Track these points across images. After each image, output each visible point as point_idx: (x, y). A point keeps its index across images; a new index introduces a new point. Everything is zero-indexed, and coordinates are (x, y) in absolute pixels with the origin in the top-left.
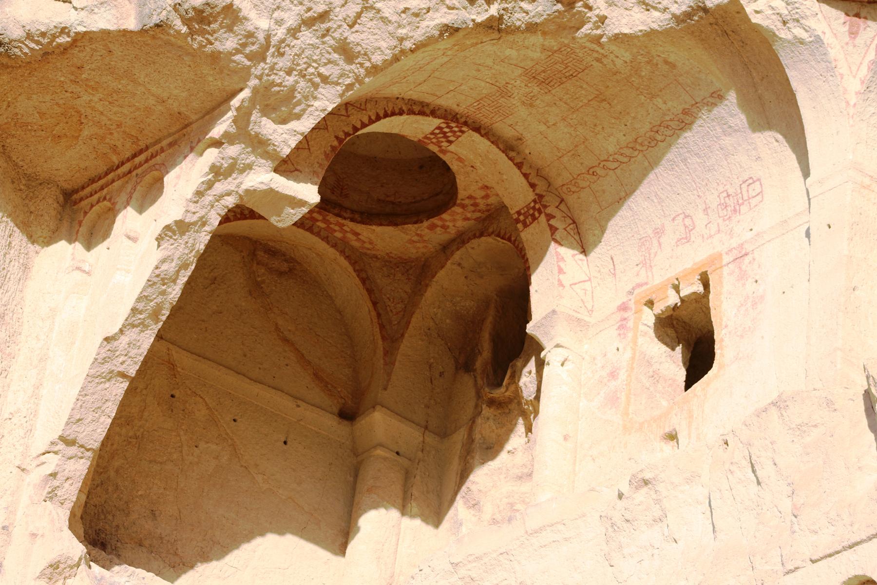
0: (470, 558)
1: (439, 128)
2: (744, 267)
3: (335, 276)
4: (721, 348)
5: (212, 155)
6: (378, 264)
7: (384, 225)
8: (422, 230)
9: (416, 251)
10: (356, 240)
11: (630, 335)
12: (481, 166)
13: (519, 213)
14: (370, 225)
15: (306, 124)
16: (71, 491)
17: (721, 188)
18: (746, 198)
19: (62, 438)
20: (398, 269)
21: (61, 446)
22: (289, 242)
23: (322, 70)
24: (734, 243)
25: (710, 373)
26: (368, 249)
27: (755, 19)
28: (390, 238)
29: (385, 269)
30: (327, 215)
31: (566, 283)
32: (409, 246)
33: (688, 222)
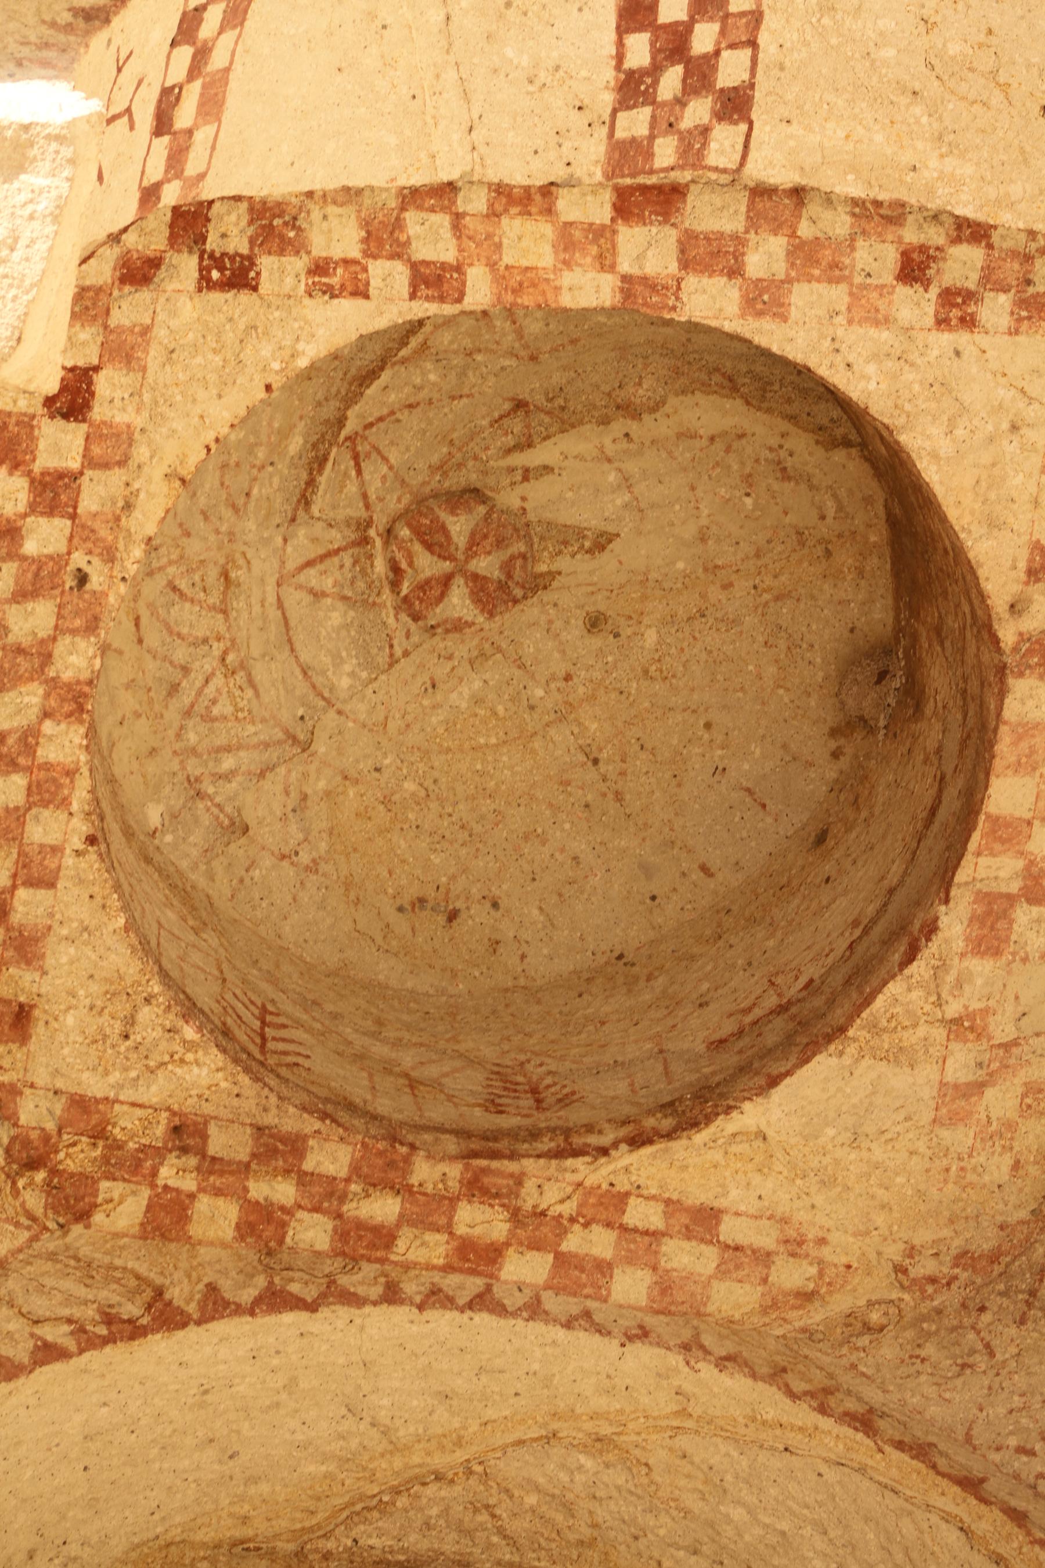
3: (738, 1514)
6: (888, 1350)
7: (788, 1073)
8: (959, 984)
9: (1008, 1160)
10: (722, 1272)
12: (950, 163)
14: (728, 1110)
20: (986, 1318)
22: (439, 1461)
26: (806, 1297)
28: (854, 1142)
29: (929, 1350)
30: (519, 1180)
32: (959, 1138)
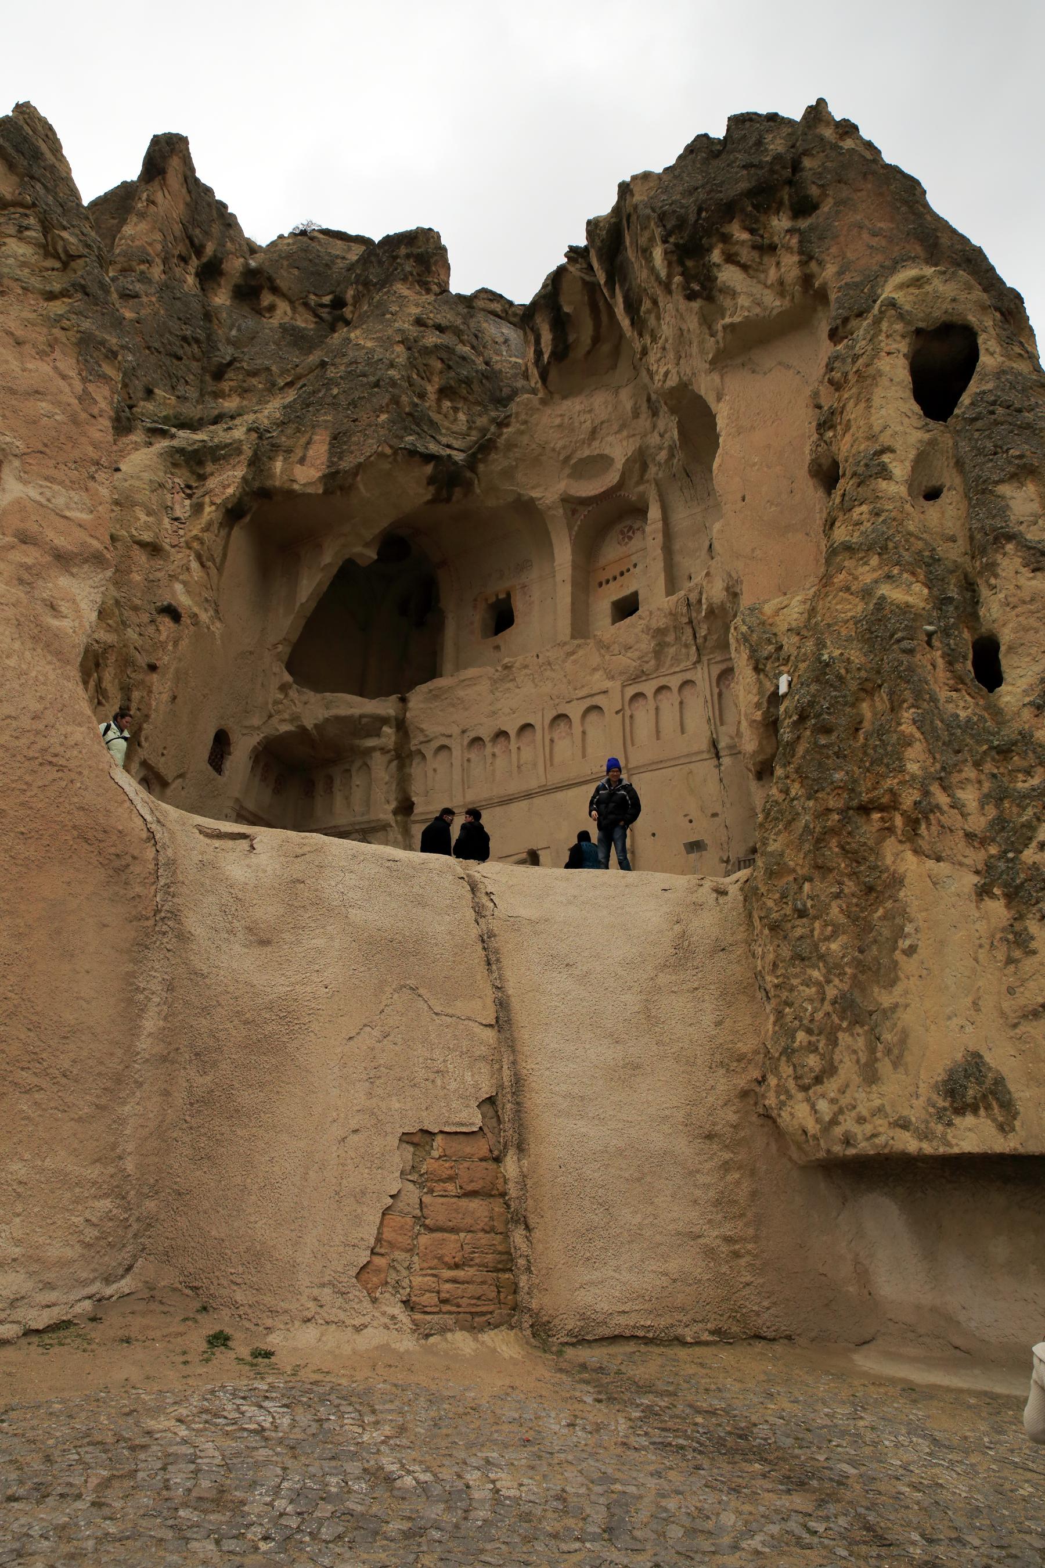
15: (377, 531)
16: (286, 658)
19: (285, 639)
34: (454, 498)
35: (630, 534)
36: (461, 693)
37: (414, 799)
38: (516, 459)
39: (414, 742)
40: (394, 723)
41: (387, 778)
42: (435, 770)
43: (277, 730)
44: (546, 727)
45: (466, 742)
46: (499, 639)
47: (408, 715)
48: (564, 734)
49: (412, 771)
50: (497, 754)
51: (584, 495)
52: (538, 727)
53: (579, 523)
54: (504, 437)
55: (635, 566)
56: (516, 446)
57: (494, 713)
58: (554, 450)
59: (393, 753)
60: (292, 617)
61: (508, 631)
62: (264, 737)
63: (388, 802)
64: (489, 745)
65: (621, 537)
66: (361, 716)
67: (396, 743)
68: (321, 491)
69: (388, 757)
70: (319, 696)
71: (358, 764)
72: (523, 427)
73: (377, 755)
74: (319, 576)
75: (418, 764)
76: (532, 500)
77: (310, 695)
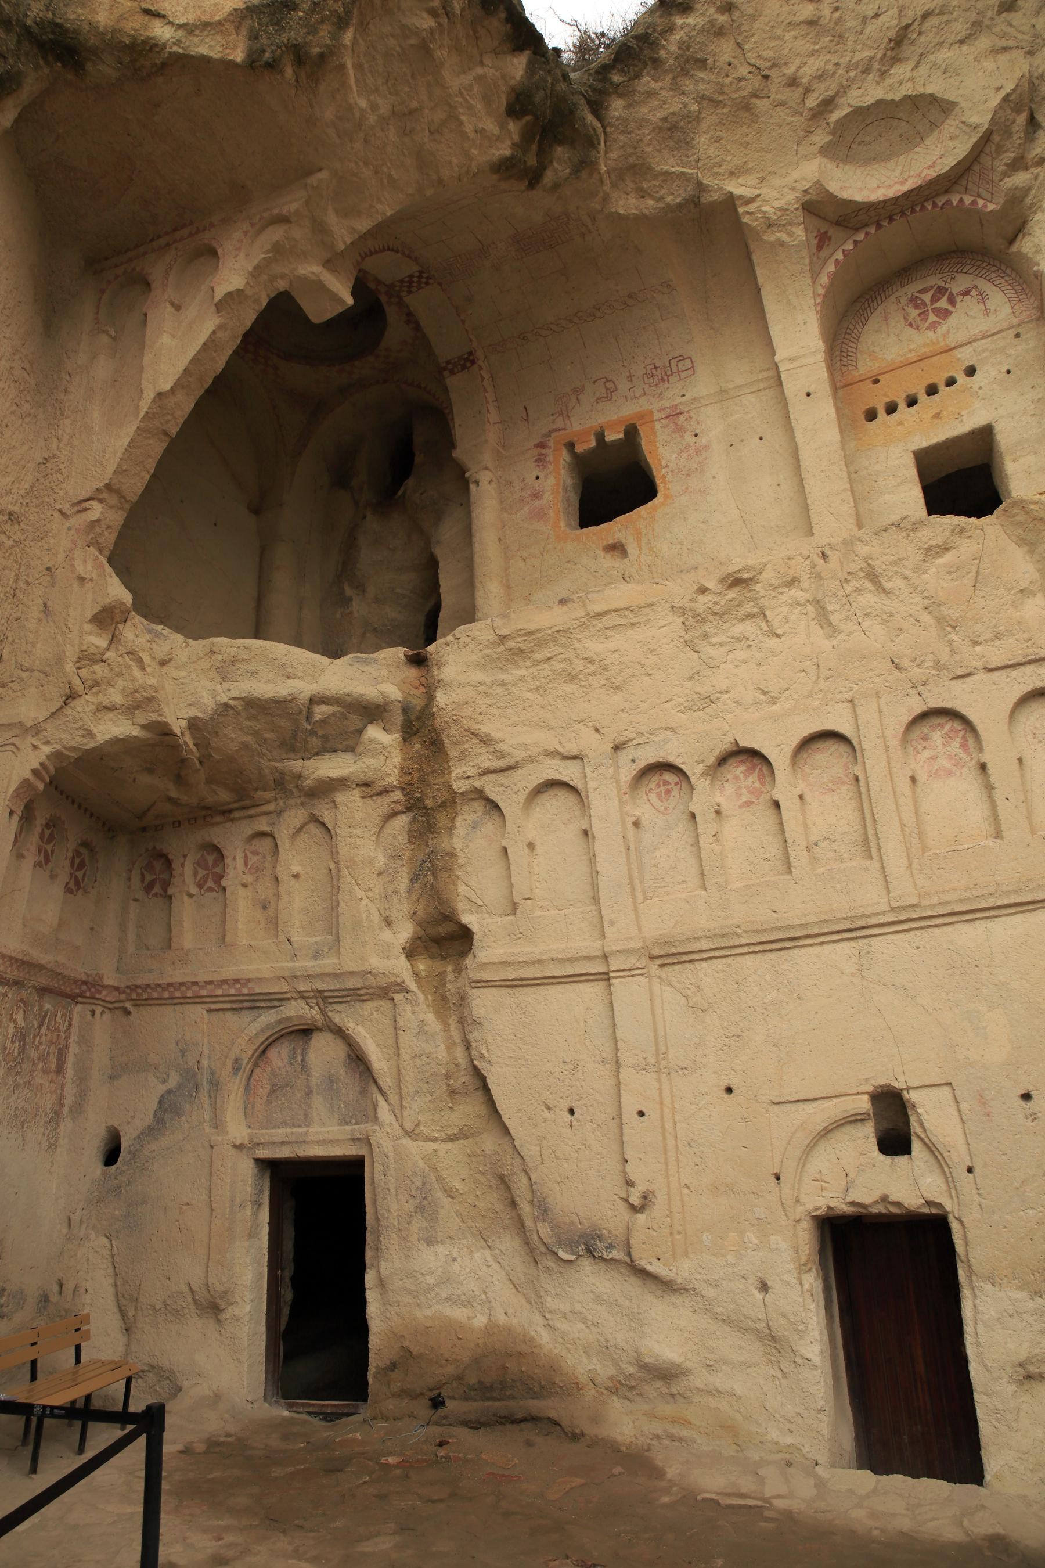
0: (521, 633)
1: (411, 276)
2: (680, 423)
4: (664, 482)
5: (276, 234)
11: (551, 467)
13: (448, 362)
16: (109, 539)
17: (648, 361)
18: (674, 370)
19: (108, 487)
21: (105, 495)
23: (393, 173)
24: (666, 403)
25: (655, 500)
27: (746, 220)
31: (492, 421)
33: (609, 385)
34: (549, 177)
35: (943, 303)
36: (595, 647)
37: (466, 919)
38: (701, 98)
39: (457, 770)
40: (398, 718)
41: (381, 861)
42: (531, 846)
43: (91, 734)
44: (894, 743)
45: (627, 772)
46: (617, 528)
47: (441, 698)
48: (948, 765)
49: (457, 843)
50: (725, 806)
51: (858, 198)
52: (869, 743)
53: (831, 268)
54: (678, 36)
55: (971, 371)
56: (702, 63)
57: (709, 700)
58: (793, 82)
59: (398, 795)
60: (130, 429)
61: (642, 510)
62: (57, 755)
63: (388, 923)
64: (702, 784)
65: (914, 313)
66: (314, 701)
67: (405, 771)
68: (239, 56)
69: (384, 805)
70: (198, 646)
71: (295, 817)
72: (722, 19)
73: (351, 800)
74: (210, 324)
75: (475, 826)
76: (731, 201)
77: (173, 641)
